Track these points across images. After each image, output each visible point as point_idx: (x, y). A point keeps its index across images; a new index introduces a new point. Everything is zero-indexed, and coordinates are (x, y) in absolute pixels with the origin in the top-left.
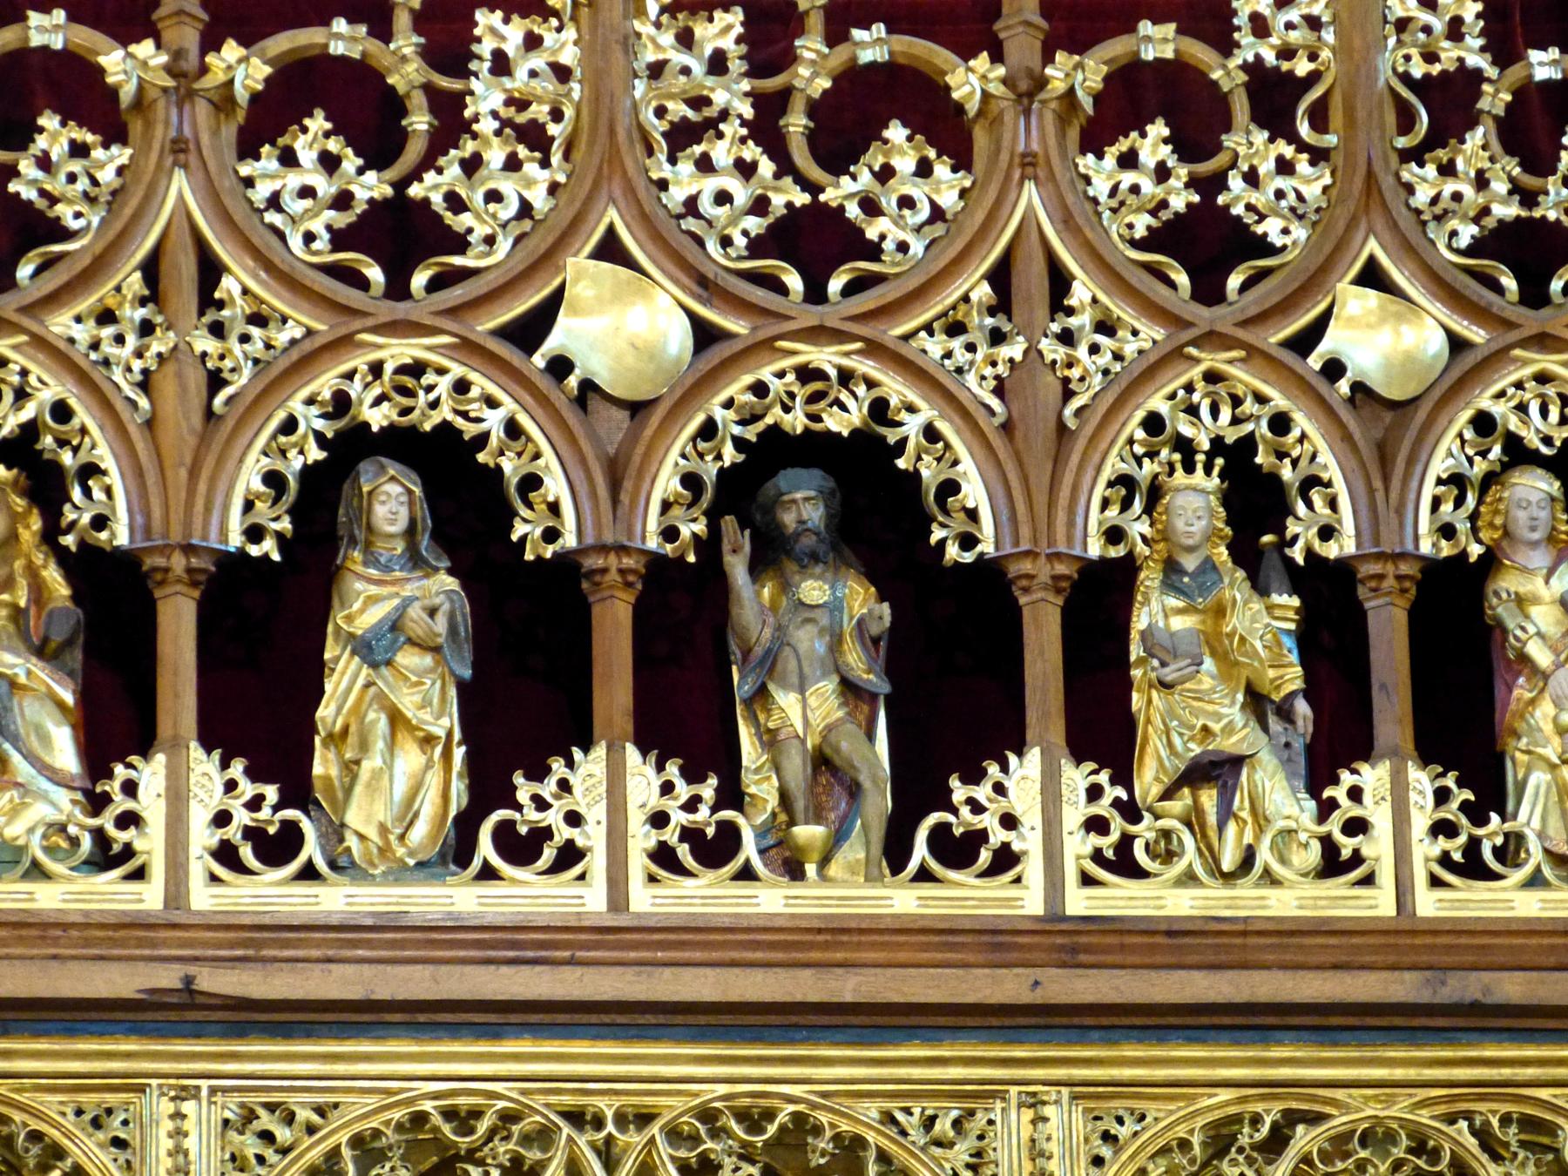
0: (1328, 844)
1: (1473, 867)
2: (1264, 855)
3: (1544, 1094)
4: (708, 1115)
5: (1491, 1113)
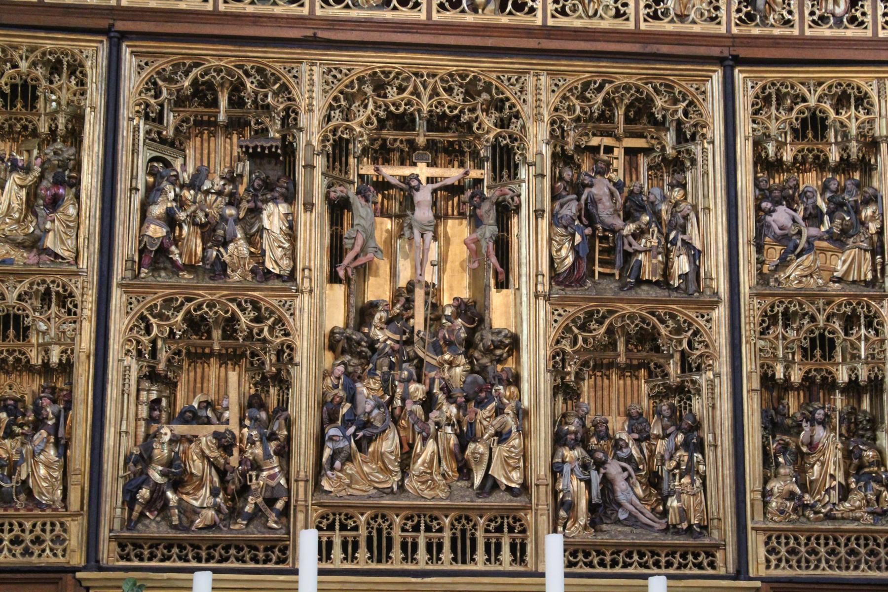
0: (617, 9)
1: (655, 17)
2: (600, 12)
3: (671, 78)
4: (451, 75)
5: (657, 83)
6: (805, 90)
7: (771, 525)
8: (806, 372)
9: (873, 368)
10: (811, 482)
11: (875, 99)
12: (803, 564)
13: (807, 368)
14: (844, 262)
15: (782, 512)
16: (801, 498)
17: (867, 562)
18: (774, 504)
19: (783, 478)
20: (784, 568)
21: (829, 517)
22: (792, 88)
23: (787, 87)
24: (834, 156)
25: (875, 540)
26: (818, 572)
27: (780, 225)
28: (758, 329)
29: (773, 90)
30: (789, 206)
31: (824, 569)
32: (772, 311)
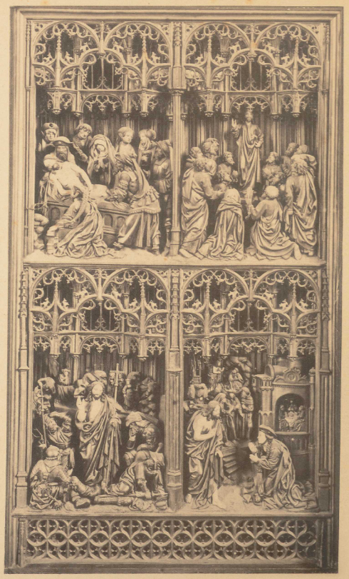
6: (94, 32)
11: (169, 45)
14: (129, 227)
23: (75, 30)
27: (64, 184)
29: (59, 34)
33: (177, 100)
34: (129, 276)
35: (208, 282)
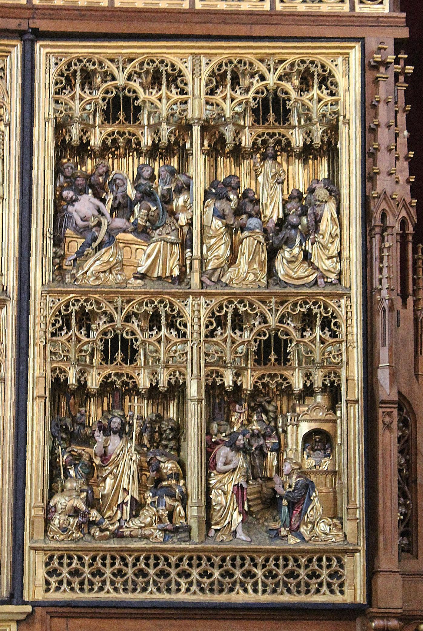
6: (113, 67)
7: (52, 544)
8: (105, 377)
9: (175, 372)
10: (103, 496)
11: (189, 78)
12: (86, 587)
13: (107, 371)
14: (149, 256)
15: (65, 530)
16: (86, 515)
17: (155, 583)
18: (56, 522)
19: (68, 493)
20: (65, 591)
21: (117, 535)
22: (100, 64)
23: (94, 64)
24: (146, 140)
25: (166, 559)
26: (102, 595)
27: (83, 216)
28: (50, 329)
30: (97, 195)
31: (108, 592)
32: (66, 310)
33: (196, 131)
34: (149, 305)
35: (230, 311)
